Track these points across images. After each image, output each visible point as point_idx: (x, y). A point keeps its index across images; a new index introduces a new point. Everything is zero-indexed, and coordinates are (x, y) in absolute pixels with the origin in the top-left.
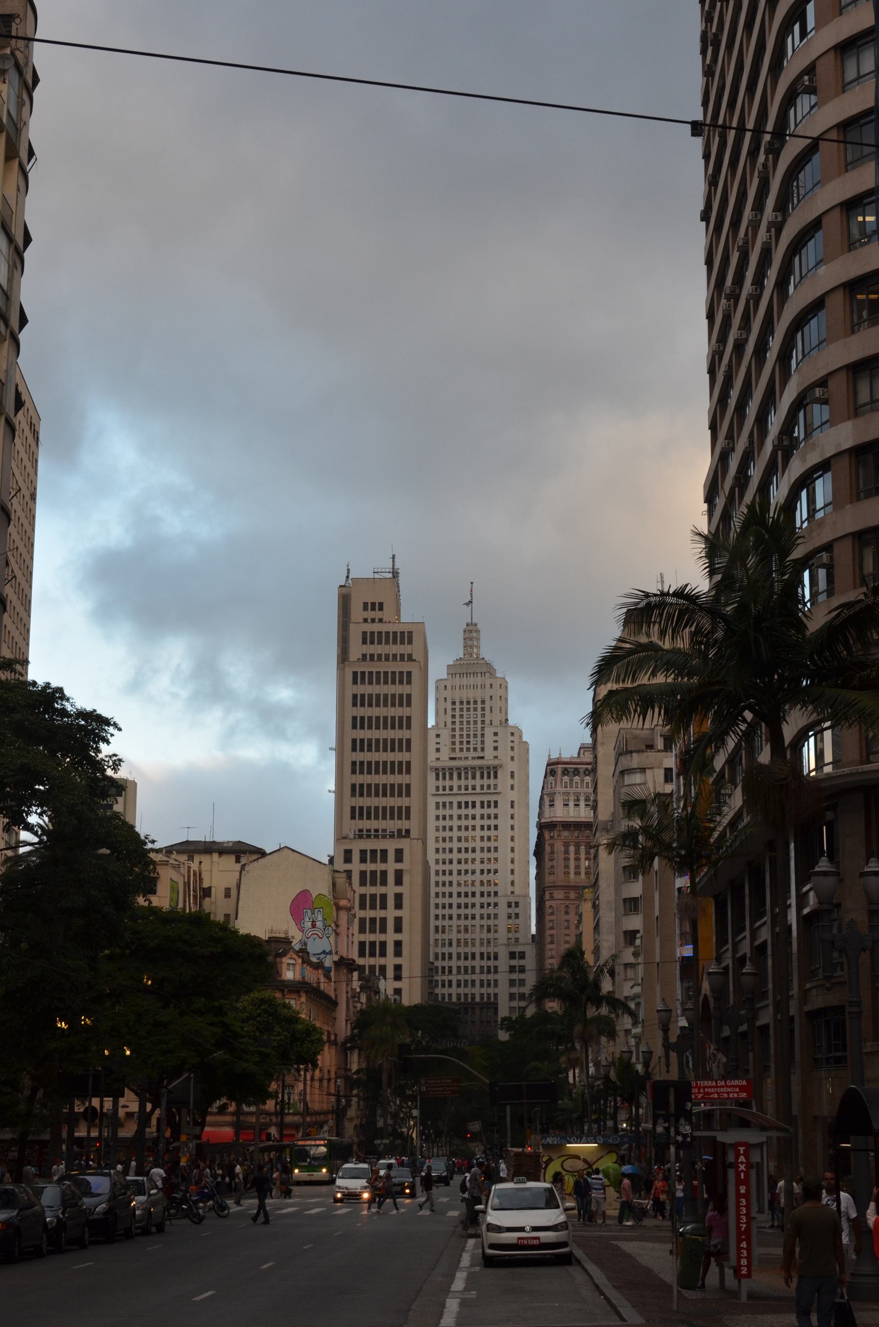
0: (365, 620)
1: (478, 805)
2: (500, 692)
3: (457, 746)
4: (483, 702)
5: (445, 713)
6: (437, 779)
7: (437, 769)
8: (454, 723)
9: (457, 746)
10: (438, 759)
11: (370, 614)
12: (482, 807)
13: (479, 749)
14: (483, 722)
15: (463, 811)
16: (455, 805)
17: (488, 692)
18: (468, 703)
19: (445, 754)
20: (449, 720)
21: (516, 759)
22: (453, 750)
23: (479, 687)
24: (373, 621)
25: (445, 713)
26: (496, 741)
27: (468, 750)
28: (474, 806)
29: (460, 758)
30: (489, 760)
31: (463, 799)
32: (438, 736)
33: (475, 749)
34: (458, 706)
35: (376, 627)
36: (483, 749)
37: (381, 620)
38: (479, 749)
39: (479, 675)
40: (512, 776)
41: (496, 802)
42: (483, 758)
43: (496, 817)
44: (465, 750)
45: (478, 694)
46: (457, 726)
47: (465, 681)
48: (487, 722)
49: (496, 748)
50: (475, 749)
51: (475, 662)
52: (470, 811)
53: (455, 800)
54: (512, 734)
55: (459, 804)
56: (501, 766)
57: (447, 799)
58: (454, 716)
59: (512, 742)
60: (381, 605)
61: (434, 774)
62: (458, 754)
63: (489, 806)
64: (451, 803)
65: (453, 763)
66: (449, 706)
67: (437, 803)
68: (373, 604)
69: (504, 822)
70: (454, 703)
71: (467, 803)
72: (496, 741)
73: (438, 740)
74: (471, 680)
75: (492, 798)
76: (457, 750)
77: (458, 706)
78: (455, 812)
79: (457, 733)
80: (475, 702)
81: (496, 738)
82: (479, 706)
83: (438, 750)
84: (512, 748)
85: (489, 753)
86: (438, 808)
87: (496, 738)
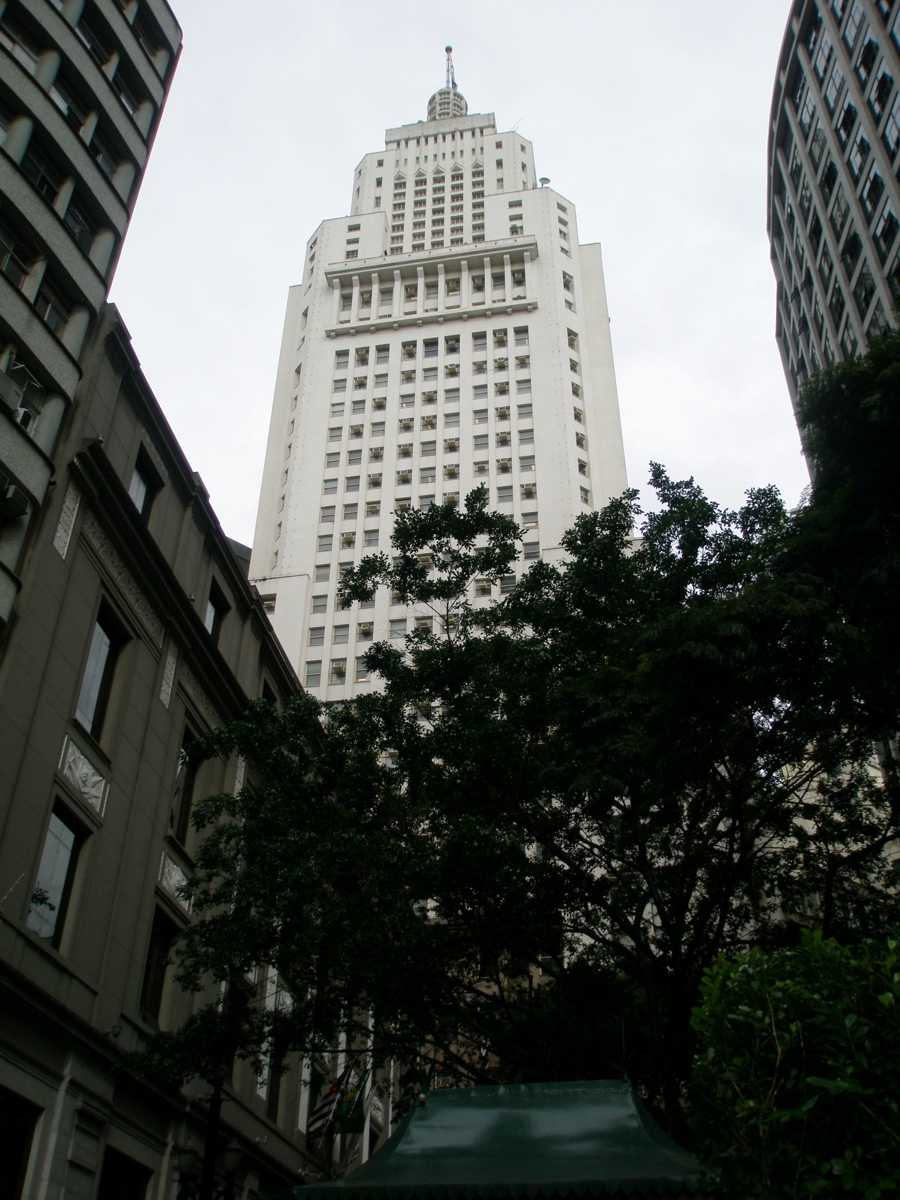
1: (466, 343)
2: (522, 157)
4: (478, 173)
7: (345, 283)
16: (396, 351)
18: (439, 179)
32: (354, 228)
34: (410, 189)
40: (567, 285)
41: (522, 331)
43: (523, 362)
47: (431, 148)
53: (395, 340)
54: (562, 208)
55: (409, 350)
56: (535, 256)
57: (372, 342)
59: (563, 222)
61: (337, 293)
64: (383, 349)
65: (391, 259)
66: (388, 191)
67: (342, 354)
70: (400, 184)
71: (431, 344)
73: (354, 235)
74: (448, 146)
77: (410, 189)
78: (396, 363)
80: (458, 176)
81: (516, 211)
87: (516, 211)
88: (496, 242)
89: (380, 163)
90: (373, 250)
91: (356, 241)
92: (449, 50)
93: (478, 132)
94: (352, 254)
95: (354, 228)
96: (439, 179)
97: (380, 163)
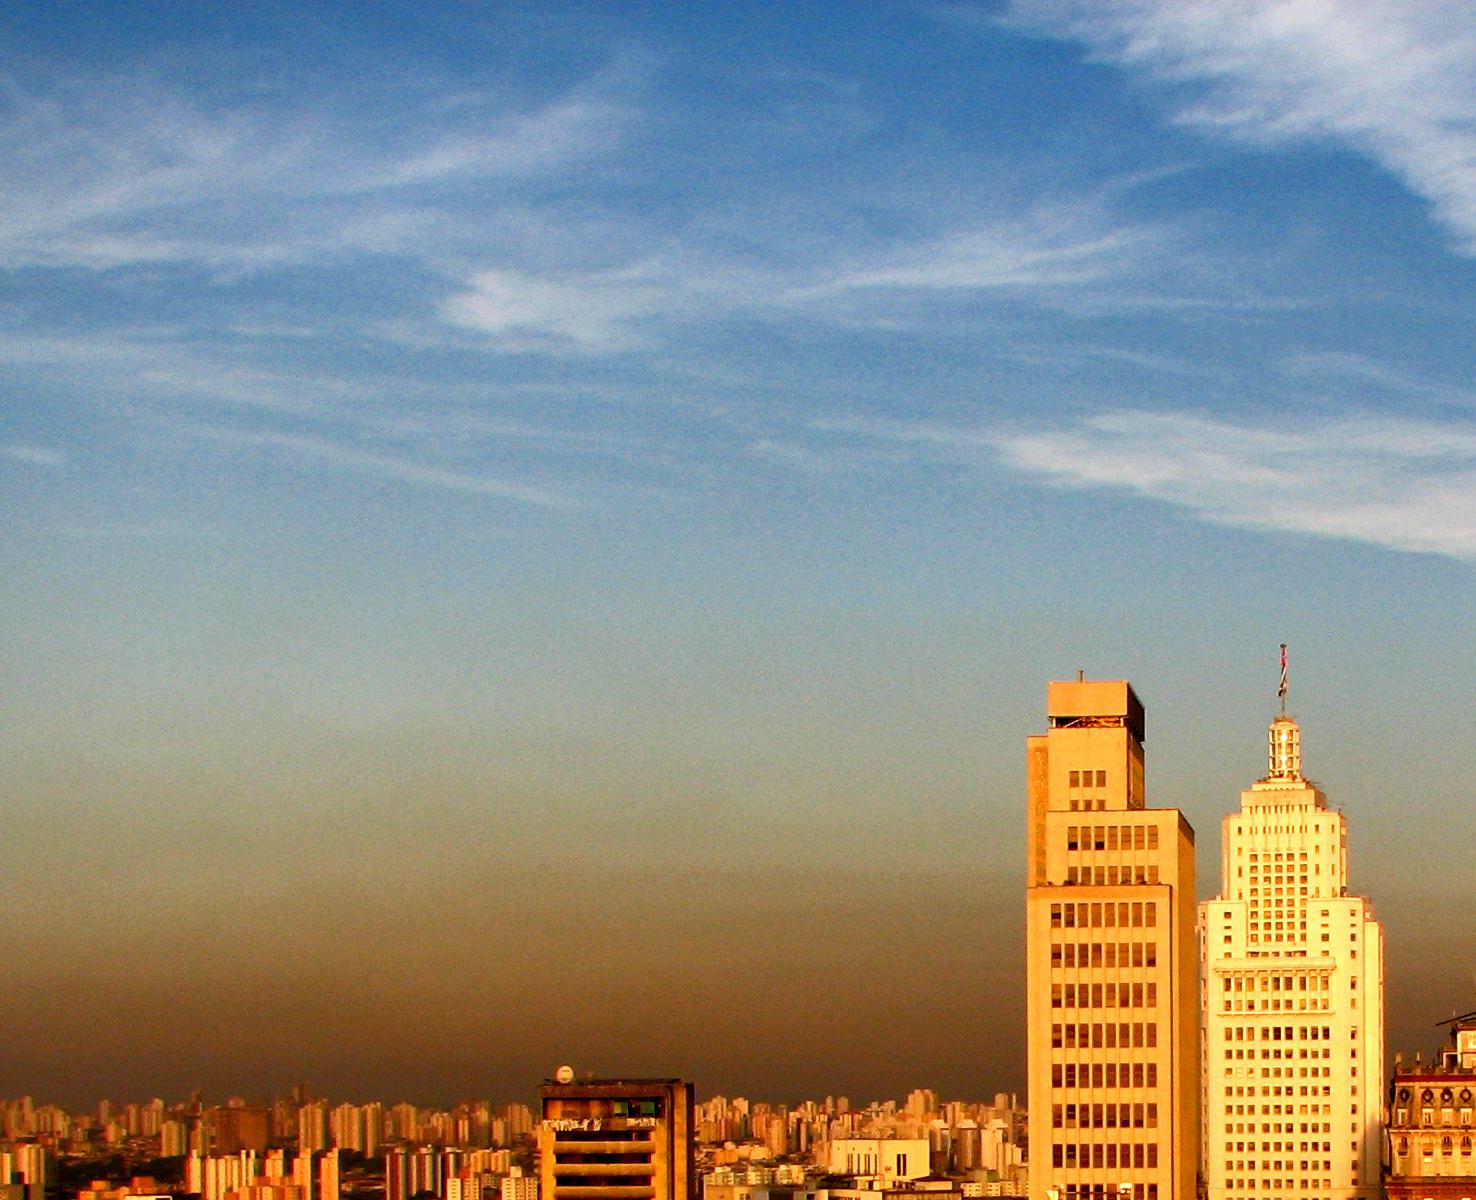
0: (1074, 806)
1: (1296, 1033)
3: (1261, 932)
4: (1304, 856)
5: (1240, 874)
6: (1228, 988)
8: (1254, 891)
9: (1261, 932)
10: (1228, 955)
11: (1081, 794)
12: (1304, 1036)
13: (1297, 938)
14: (1304, 891)
15: (1272, 1045)
16: (1258, 1033)
17: (1312, 839)
19: (1240, 947)
20: (1246, 888)
21: (1359, 955)
22: (1254, 938)
23: (1297, 830)
24: (1088, 806)
25: (1240, 874)
26: (1325, 925)
27: (1279, 938)
28: (1289, 1036)
29: (1265, 954)
30: (1314, 959)
31: (1271, 1025)
33: (1291, 937)
34: (1261, 863)
35: (1092, 819)
36: (1303, 937)
37: (1102, 805)
38: (1297, 938)
39: (1297, 808)
42: (1304, 953)
43: (1326, 1054)
44: (1274, 938)
45: (1294, 843)
46: (1261, 898)
47: (1272, 819)
48: (1311, 891)
49: (1325, 938)
50: (1291, 937)
51: (1291, 786)
52: (1283, 1045)
58: (1254, 880)
60: (1102, 775)
62: (1261, 946)
63: (1315, 1036)
66: (1246, 864)
68: (1088, 774)
69: (1339, 1063)
70: (1254, 857)
71: (1277, 1031)
72: (1325, 925)
73: (1228, 922)
74: (1284, 819)
75: (1320, 1024)
76: (1261, 938)
79: (1261, 909)
80: (1290, 856)
81: (1325, 920)
82: (1297, 862)
83: (1228, 939)
84: (1353, 937)
85: (1314, 946)
86: (1229, 1037)
88: (1313, 959)
89: (1240, 829)
90: (1241, 962)
91: (1229, 928)
92: (1283, 646)
93: (1304, 807)
94: (1228, 939)
95: (1228, 915)
96: (1278, 856)
97: (1240, 829)
